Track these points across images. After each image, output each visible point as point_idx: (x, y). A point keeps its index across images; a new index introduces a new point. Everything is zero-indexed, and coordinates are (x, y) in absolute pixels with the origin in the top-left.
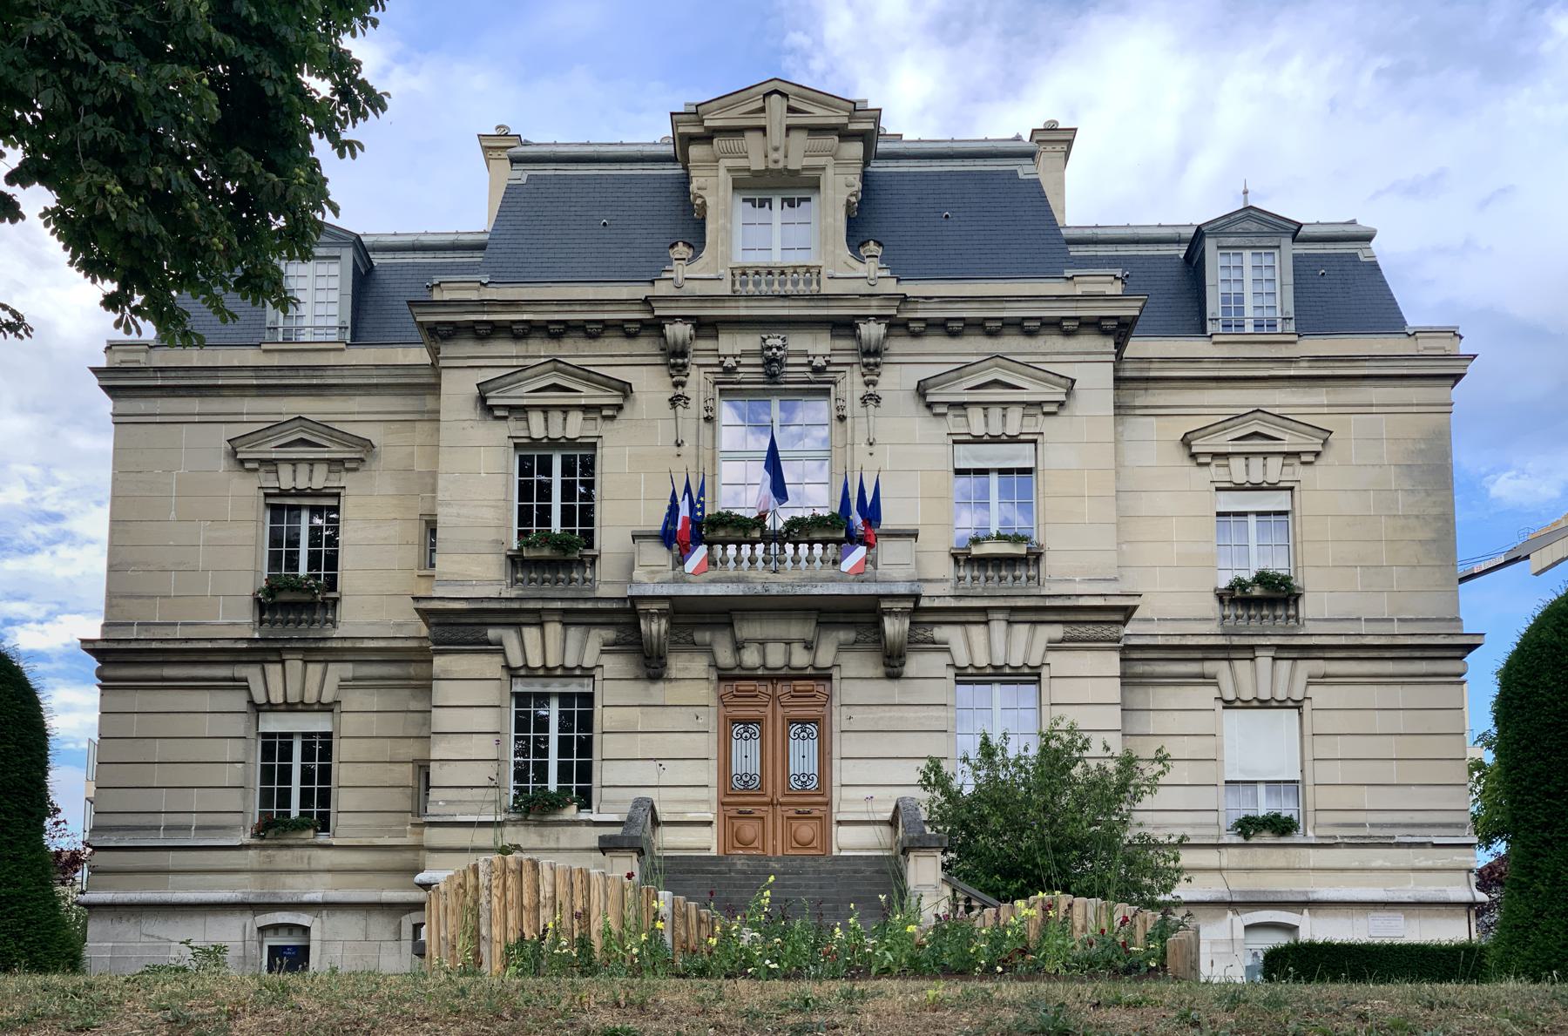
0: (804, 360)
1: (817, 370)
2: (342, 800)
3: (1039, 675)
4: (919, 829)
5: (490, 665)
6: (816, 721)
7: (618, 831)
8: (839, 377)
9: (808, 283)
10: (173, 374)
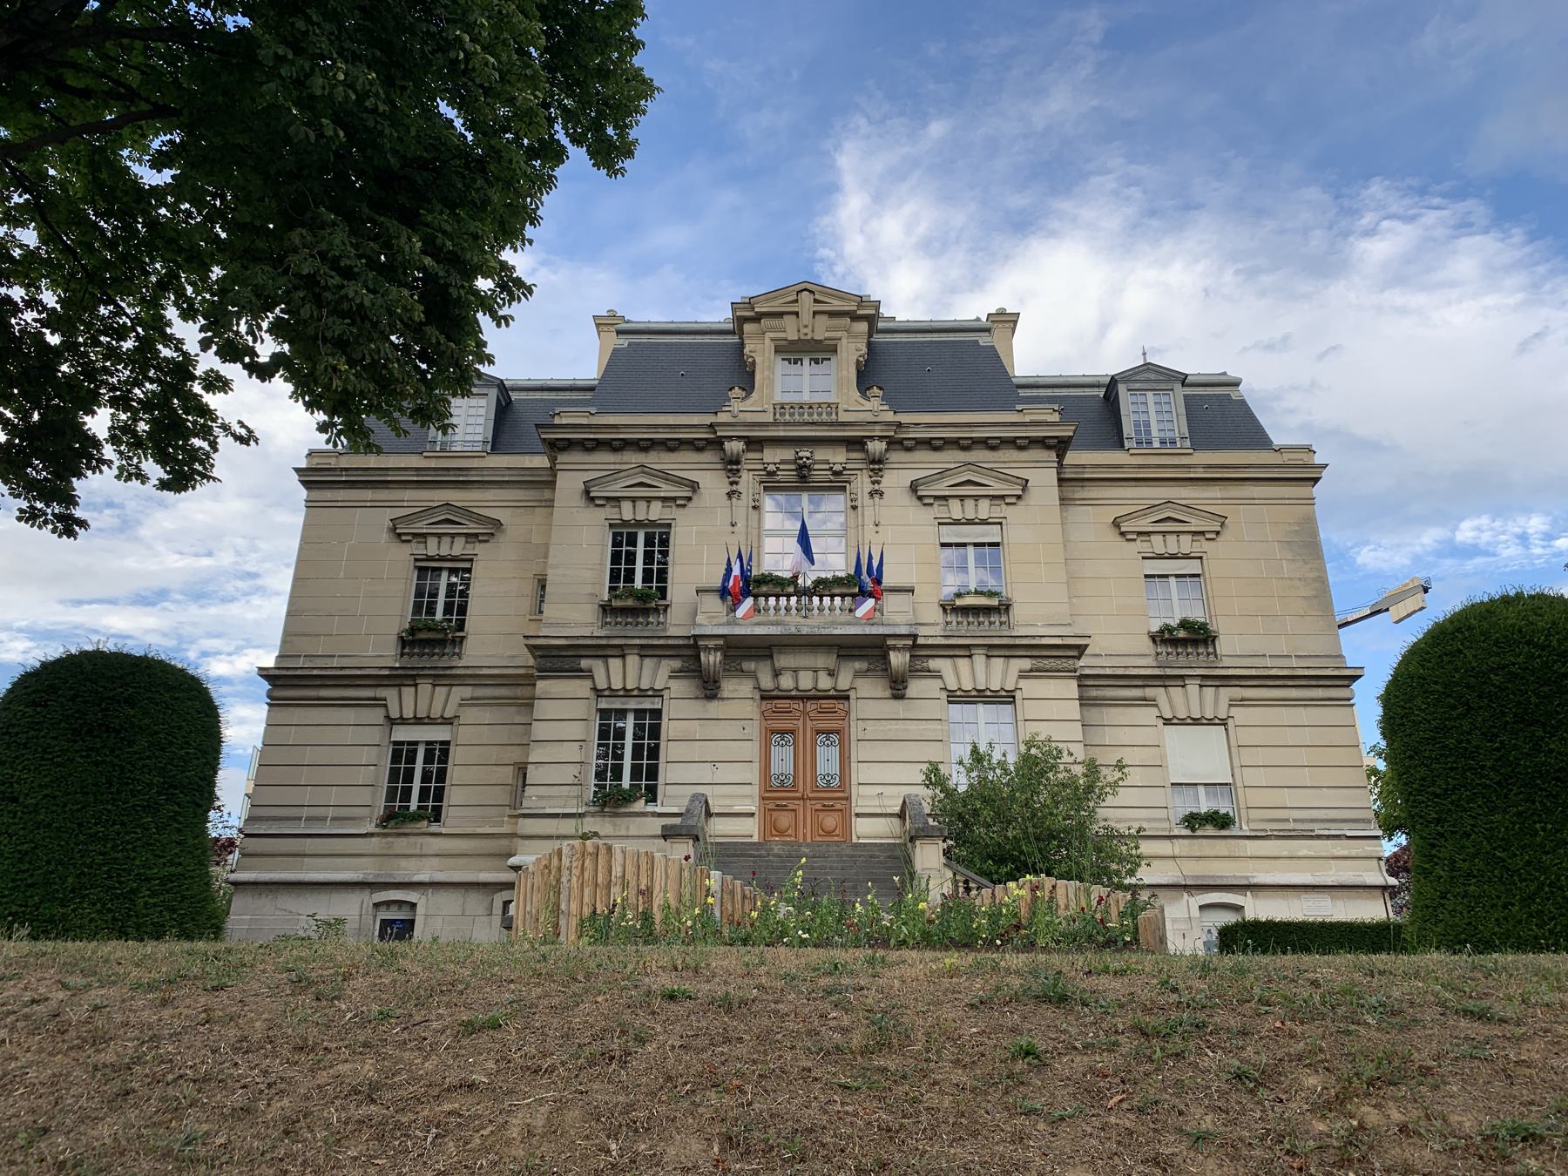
0: (827, 467)
1: (836, 473)
3: (1014, 697)
4: (922, 820)
5: (581, 688)
6: (838, 732)
7: (677, 821)
8: (852, 478)
9: (829, 414)
10: (355, 473)
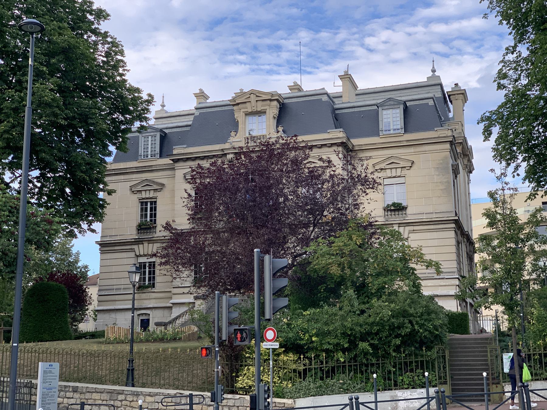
2: (158, 279)
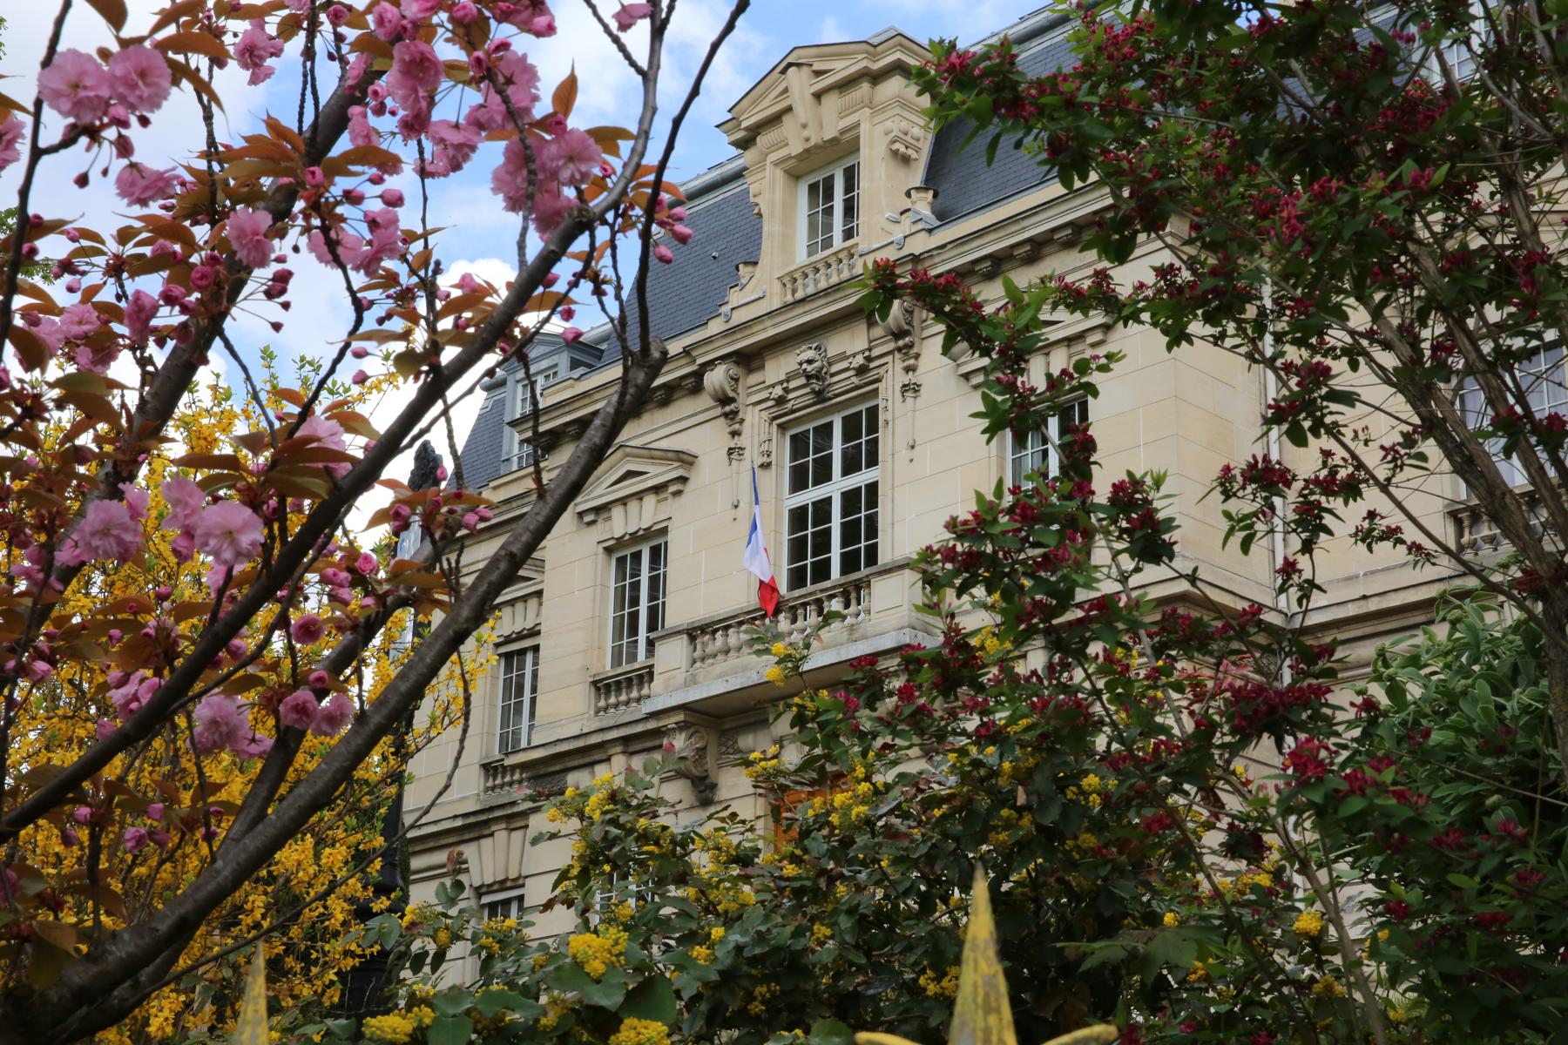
8: (882, 371)
